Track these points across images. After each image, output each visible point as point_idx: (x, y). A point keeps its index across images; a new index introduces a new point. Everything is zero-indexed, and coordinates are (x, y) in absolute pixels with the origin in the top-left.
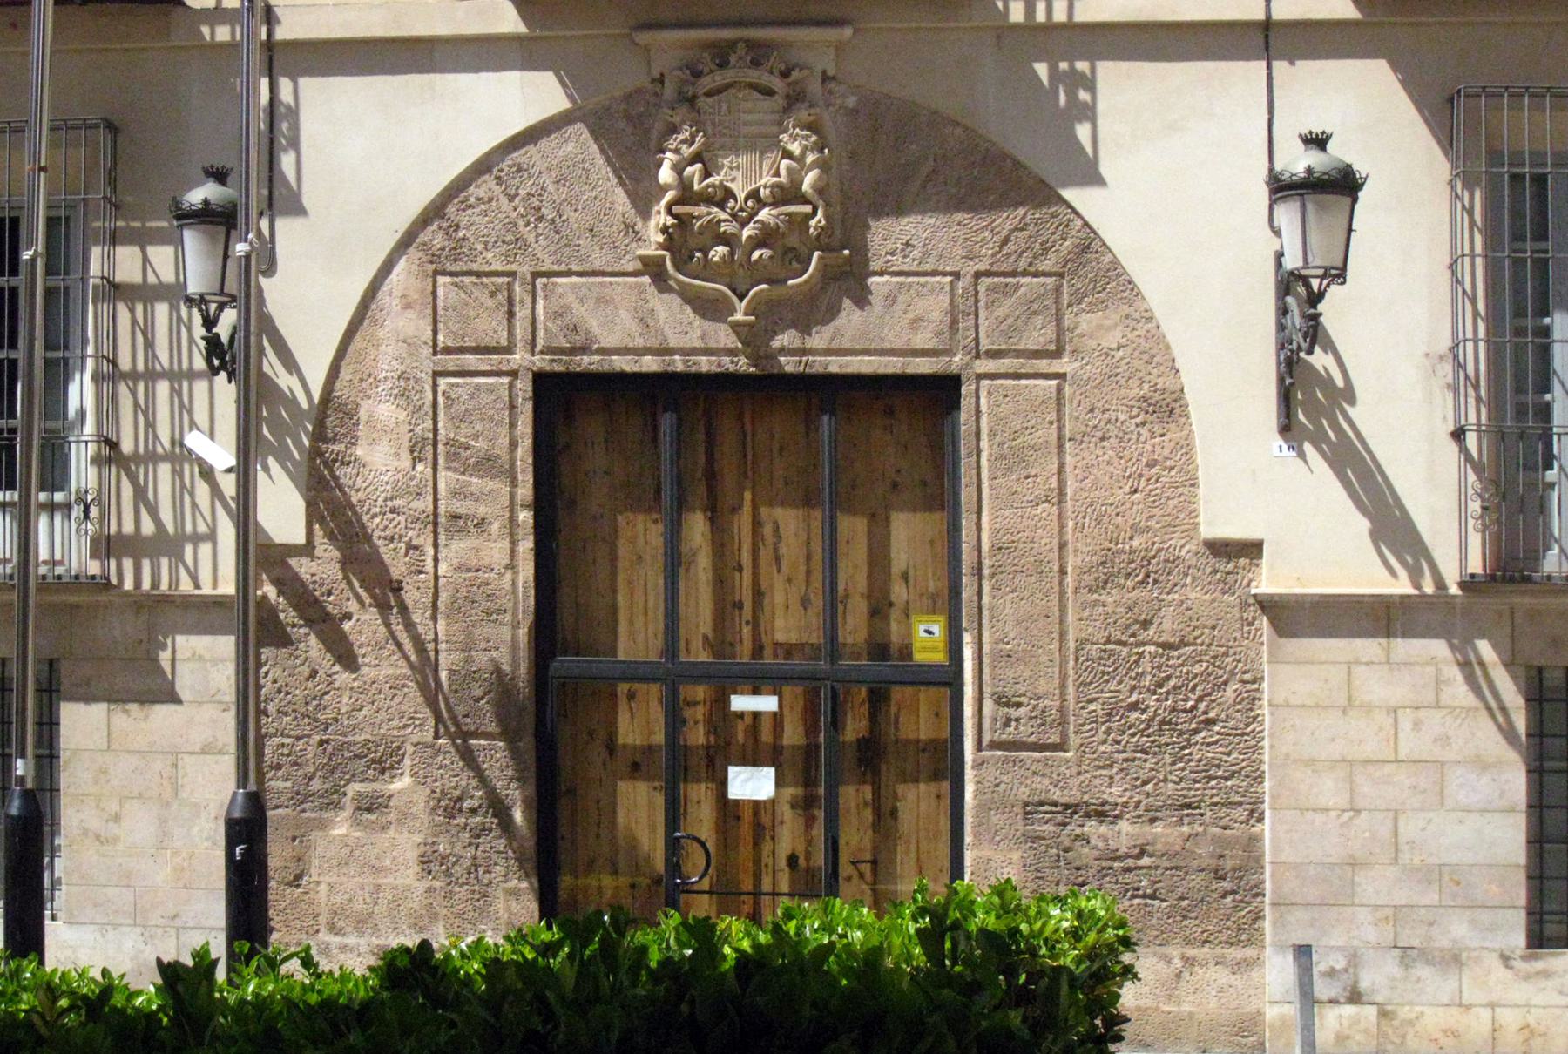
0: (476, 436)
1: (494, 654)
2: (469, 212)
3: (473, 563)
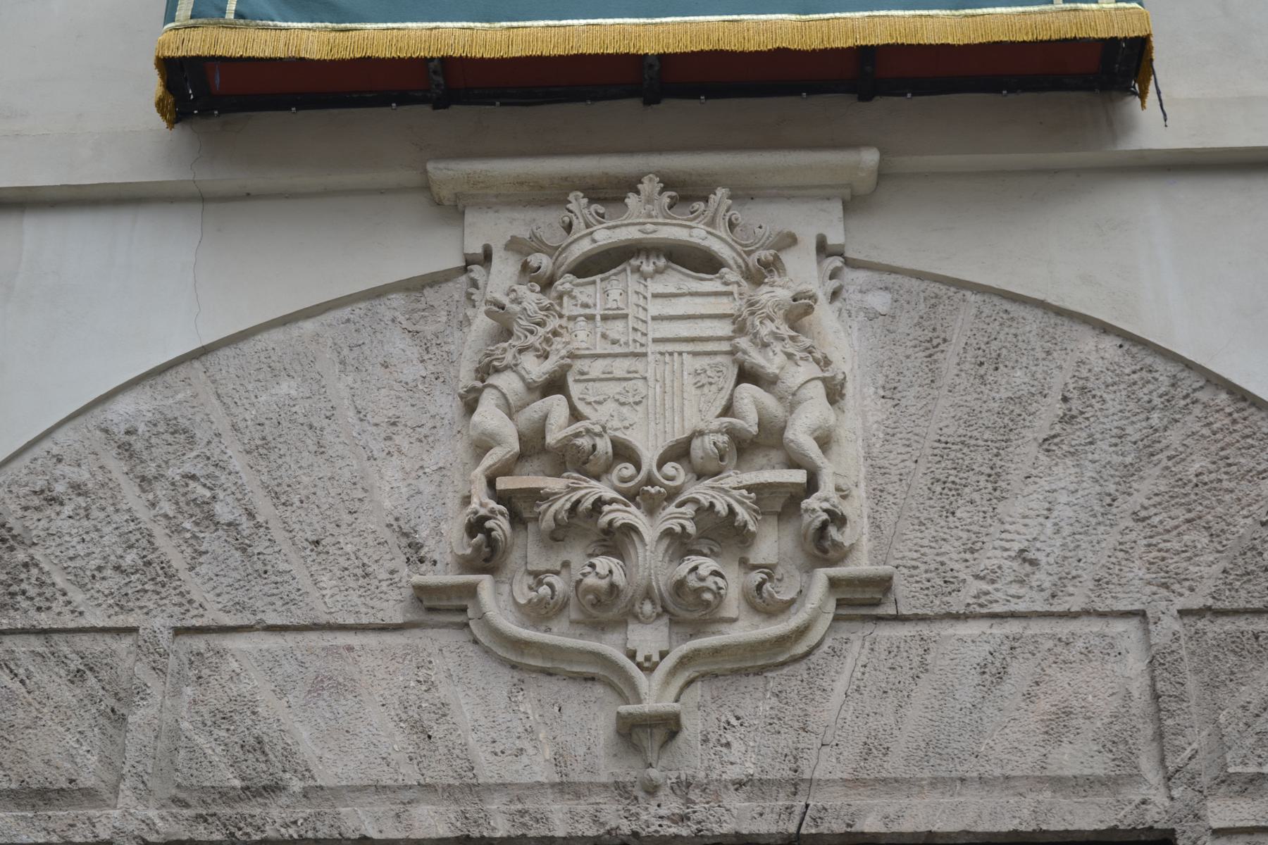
2: (49, 512)
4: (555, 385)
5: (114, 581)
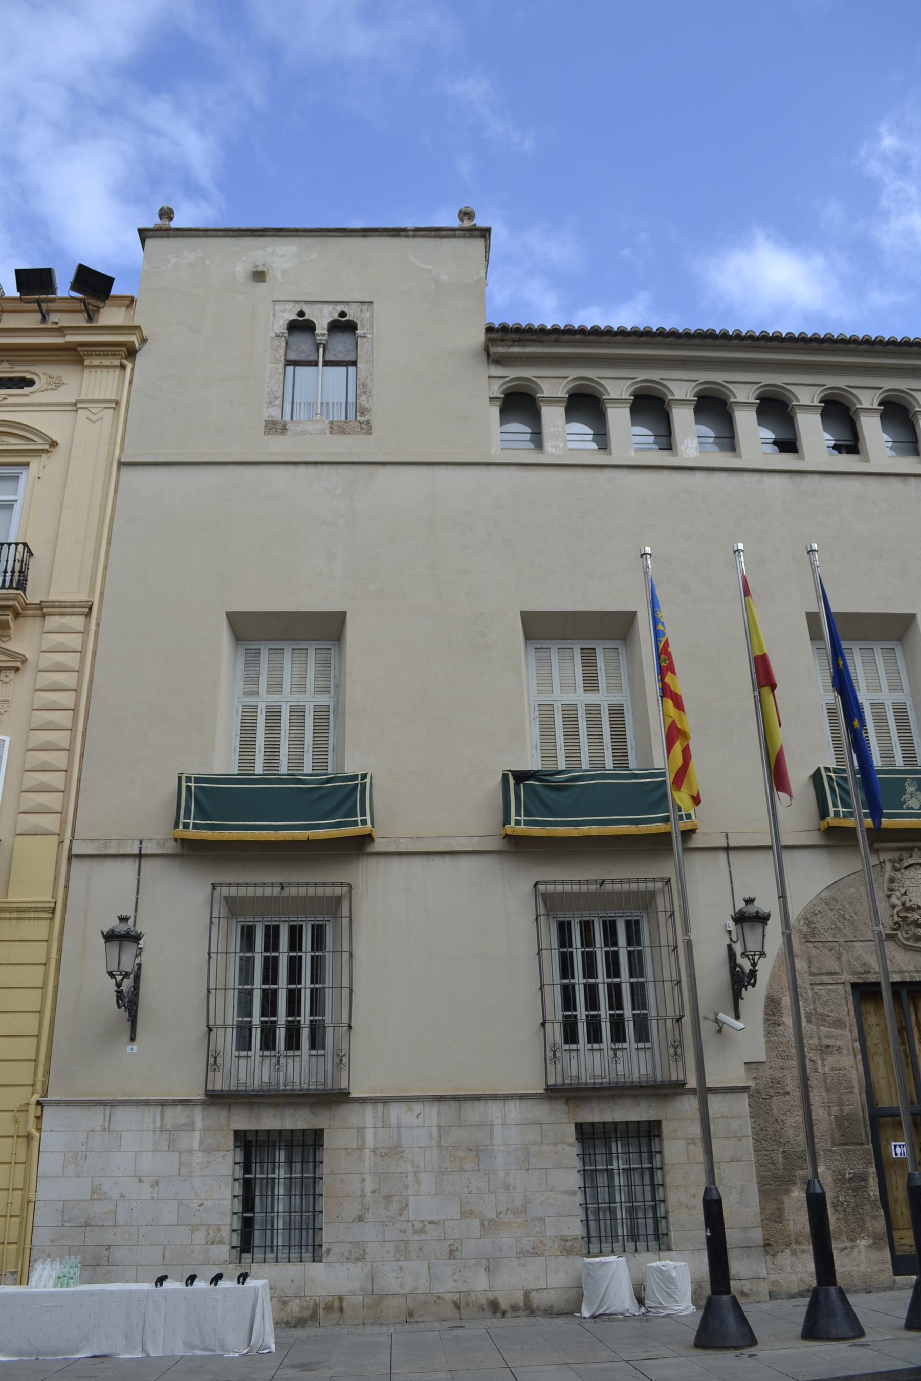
0: (832, 1011)
1: (852, 1107)
3: (838, 1066)
4: (905, 894)
5: (831, 931)
